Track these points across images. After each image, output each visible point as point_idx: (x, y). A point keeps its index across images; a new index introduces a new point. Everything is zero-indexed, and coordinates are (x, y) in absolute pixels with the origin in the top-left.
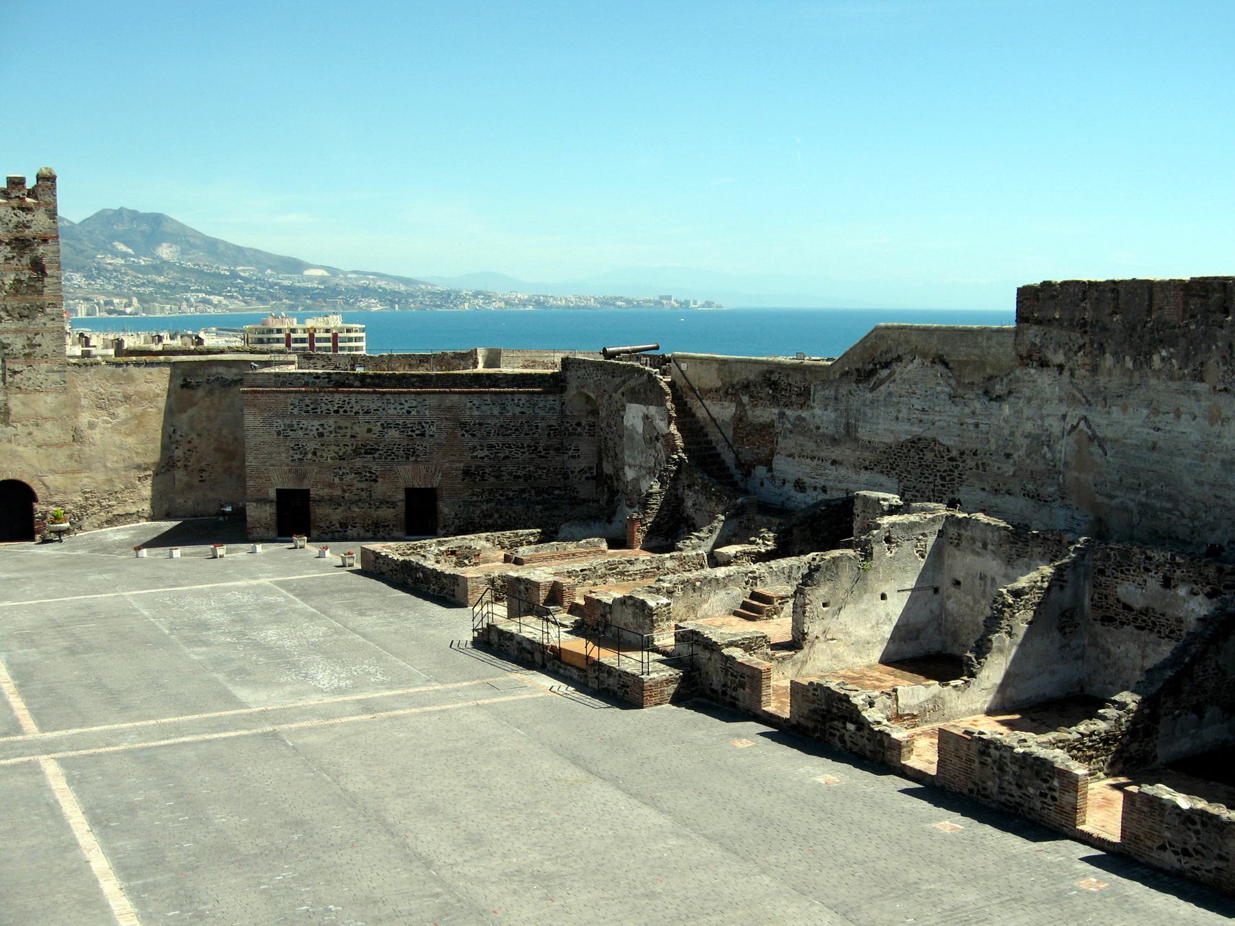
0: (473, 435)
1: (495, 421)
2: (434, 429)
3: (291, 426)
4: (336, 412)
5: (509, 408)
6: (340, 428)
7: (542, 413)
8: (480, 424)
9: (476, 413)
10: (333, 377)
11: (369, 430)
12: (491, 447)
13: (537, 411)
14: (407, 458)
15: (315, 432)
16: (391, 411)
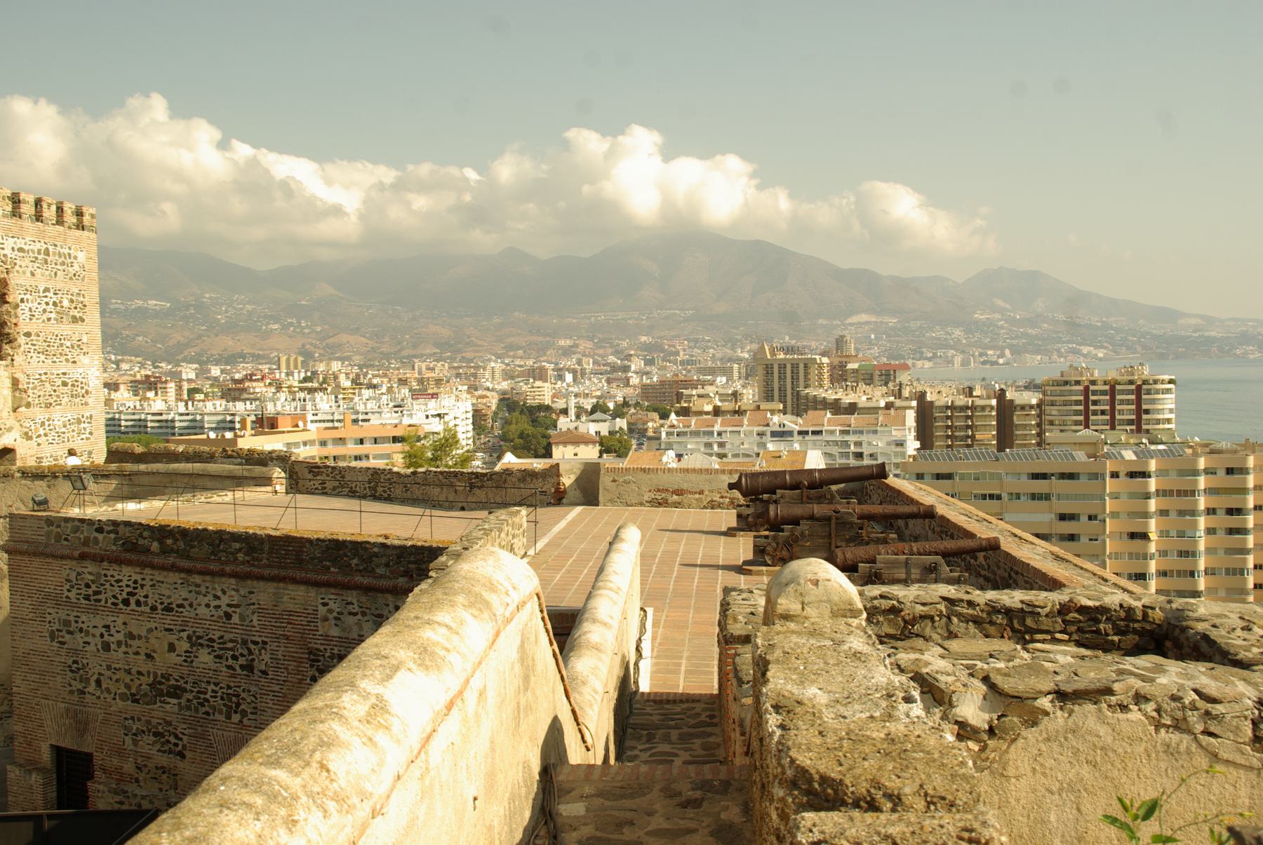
2: (266, 657)
3: (67, 623)
4: (126, 602)
6: (131, 636)
10: (121, 529)
11: (172, 648)
14: (229, 717)
15: (99, 640)
16: (202, 611)
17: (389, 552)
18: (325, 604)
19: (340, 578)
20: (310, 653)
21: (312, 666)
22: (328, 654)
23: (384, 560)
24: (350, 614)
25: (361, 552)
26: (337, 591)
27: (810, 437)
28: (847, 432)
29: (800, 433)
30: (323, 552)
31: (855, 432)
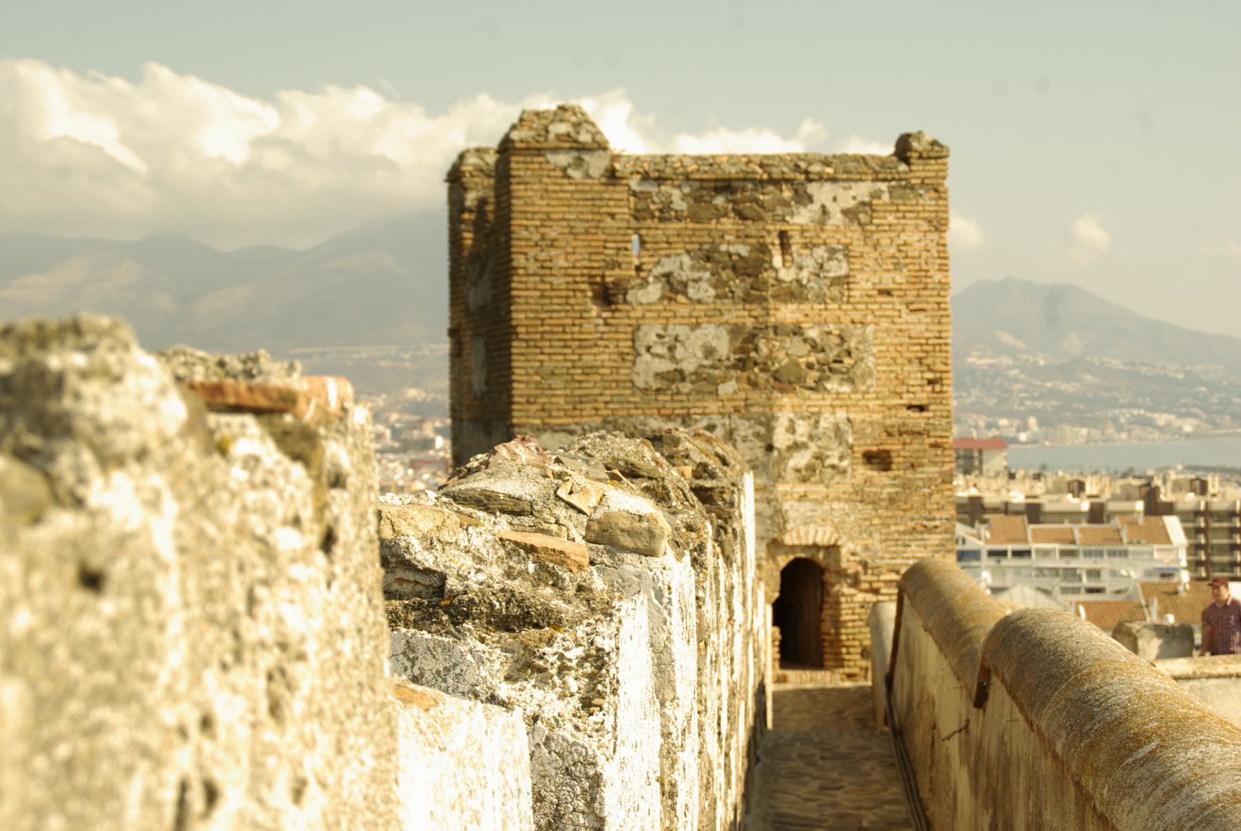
27: (1009, 562)
28: (1072, 554)
29: (992, 554)
31: (1088, 554)
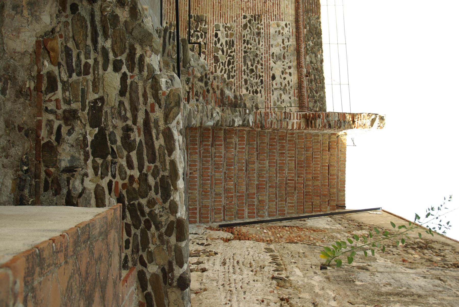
0: (245, 26)
1: (262, 48)
5: (279, 63)
7: (274, 97)
8: (259, 34)
9: (272, 31)
12: (231, 44)
13: (276, 93)
17: (319, 64)
18: (286, 25)
19: (302, 35)
20: (259, 16)
21: (252, 16)
22: (260, 26)
23: (314, 60)
24: (283, 40)
25: (317, 47)
26: (294, 33)
30: (313, 25)
